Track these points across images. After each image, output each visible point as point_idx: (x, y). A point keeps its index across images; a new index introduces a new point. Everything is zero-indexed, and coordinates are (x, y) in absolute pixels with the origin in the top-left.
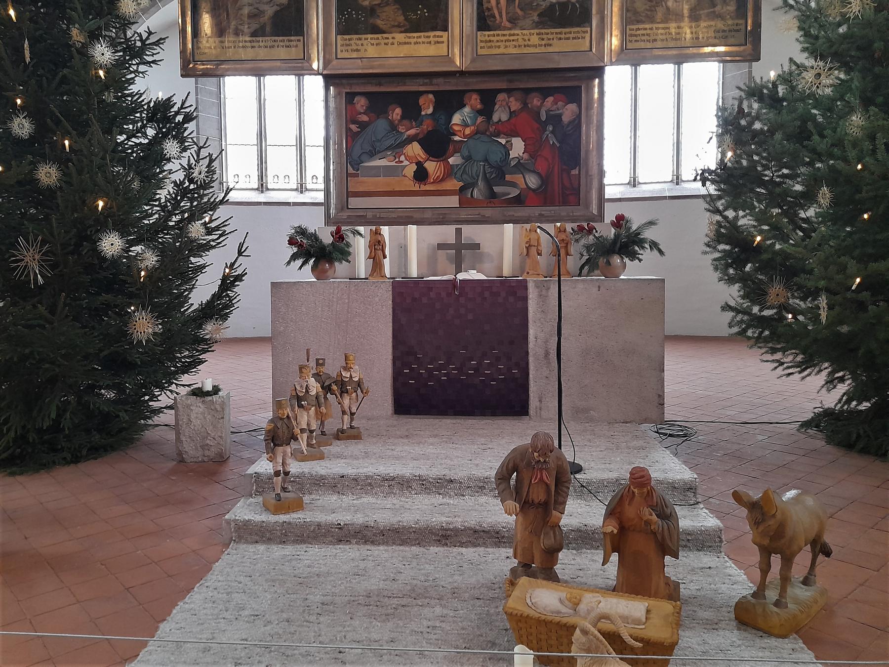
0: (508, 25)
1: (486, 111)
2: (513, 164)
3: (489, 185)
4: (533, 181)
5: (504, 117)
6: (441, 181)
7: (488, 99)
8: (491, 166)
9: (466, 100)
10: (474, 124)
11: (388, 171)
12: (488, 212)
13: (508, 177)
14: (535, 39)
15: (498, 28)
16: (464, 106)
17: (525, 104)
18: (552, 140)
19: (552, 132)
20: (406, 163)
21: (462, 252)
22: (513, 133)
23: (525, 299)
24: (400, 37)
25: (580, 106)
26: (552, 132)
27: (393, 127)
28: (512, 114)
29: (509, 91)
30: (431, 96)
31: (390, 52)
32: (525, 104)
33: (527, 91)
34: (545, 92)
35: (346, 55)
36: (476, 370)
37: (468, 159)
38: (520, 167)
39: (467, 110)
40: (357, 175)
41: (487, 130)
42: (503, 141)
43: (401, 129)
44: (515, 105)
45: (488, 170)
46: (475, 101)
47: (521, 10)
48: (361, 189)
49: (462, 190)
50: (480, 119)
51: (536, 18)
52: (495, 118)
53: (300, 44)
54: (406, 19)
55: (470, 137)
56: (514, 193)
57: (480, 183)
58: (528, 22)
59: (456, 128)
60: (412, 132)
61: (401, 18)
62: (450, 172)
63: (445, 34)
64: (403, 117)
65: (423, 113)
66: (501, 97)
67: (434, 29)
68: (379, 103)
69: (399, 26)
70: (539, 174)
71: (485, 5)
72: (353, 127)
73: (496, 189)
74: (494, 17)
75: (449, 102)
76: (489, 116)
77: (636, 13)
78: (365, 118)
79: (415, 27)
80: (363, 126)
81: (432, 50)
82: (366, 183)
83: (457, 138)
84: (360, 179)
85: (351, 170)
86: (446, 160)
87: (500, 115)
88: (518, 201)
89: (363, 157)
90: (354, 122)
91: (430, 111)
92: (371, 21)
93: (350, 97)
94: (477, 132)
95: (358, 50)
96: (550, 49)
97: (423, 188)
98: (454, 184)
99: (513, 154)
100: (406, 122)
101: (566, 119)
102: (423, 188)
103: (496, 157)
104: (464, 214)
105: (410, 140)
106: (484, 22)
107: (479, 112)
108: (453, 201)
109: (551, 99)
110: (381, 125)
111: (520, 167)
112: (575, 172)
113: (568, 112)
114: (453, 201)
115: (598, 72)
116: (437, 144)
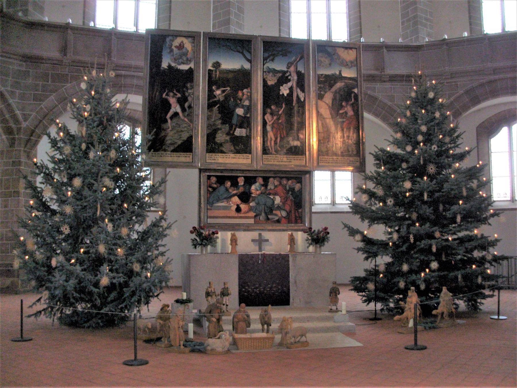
0: (275, 153)
2: (276, 206)
3: (266, 214)
4: (284, 214)
5: (273, 188)
6: (247, 212)
7: (266, 180)
8: (267, 207)
9: (257, 180)
10: (260, 189)
13: (274, 212)
14: (285, 159)
15: (271, 154)
18: (291, 197)
19: (292, 194)
20: (232, 205)
21: (260, 242)
22: (276, 194)
23: (288, 261)
24: (232, 155)
25: (301, 185)
26: (292, 194)
27: (227, 190)
28: (276, 187)
29: (274, 178)
30: (243, 178)
31: (228, 161)
32: (280, 183)
33: (281, 178)
34: (288, 179)
35: (210, 161)
36: (271, 288)
37: (258, 204)
38: (279, 208)
39: (257, 184)
40: (211, 209)
41: (266, 193)
42: (272, 197)
43: (230, 190)
45: (266, 208)
46: (260, 181)
47: (280, 147)
48: (212, 215)
49: (256, 216)
50: (263, 188)
51: (285, 151)
52: (269, 188)
53: (191, 156)
54: (235, 149)
55: (259, 195)
56: (276, 218)
57: (263, 214)
58: (282, 152)
59: (253, 191)
60: (235, 192)
61: (233, 148)
62: (251, 209)
63: (250, 155)
64: (231, 186)
65: (239, 184)
66: (271, 180)
67: (246, 153)
68: (221, 180)
69: (232, 151)
70: (287, 211)
71: (266, 145)
72: (210, 189)
73: (270, 217)
74: (269, 149)
75: (250, 181)
77: (322, 152)
78: (215, 186)
79: (238, 152)
80: (214, 189)
81: (245, 161)
82: (216, 213)
83: (253, 195)
84: (213, 211)
85: (209, 207)
86: (249, 203)
87: (270, 186)
88: (278, 221)
89: (215, 201)
90: (210, 187)
91: (242, 184)
92: (221, 148)
93: (209, 177)
94: (261, 193)
95: (215, 160)
96: (291, 163)
97: (240, 215)
98: (252, 214)
99: (276, 202)
100: (232, 188)
102: (240, 215)
103: (269, 203)
106: (265, 151)
107: (263, 185)
108: (252, 221)
109: (290, 181)
110: (222, 189)
111: (279, 208)
112: (300, 210)
113: (297, 187)
114: (252, 221)
115: (309, 173)
116: (245, 197)
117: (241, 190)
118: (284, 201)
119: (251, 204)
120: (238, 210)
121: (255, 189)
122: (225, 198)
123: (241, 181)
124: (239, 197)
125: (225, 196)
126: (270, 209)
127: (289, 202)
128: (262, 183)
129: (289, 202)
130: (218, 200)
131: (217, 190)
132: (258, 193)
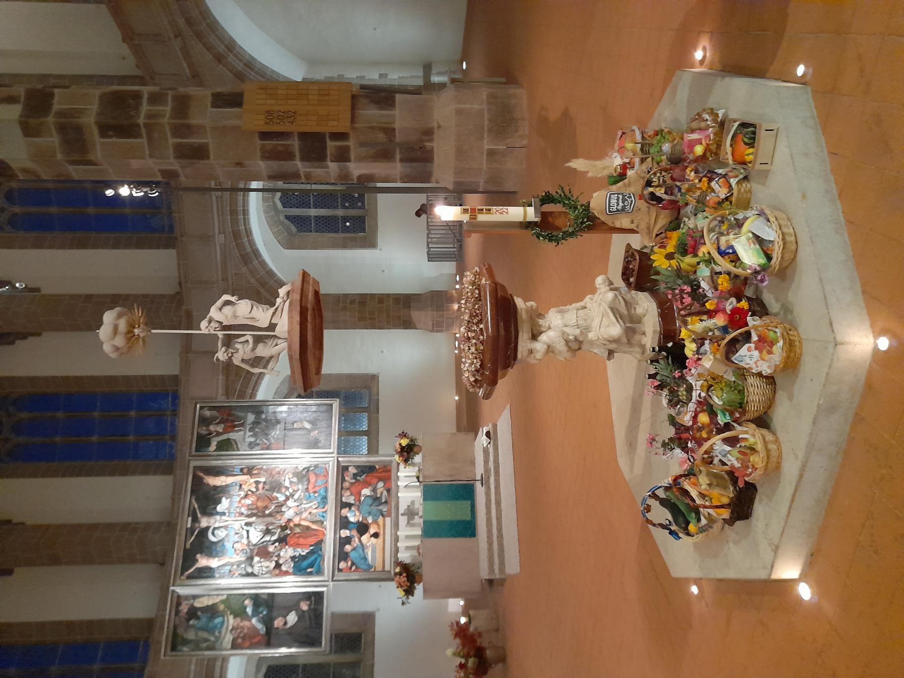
1: (349, 505)
4: (381, 484)
5: (353, 498)
11: (374, 551)
12: (393, 504)
16: (346, 517)
17: (348, 489)
18: (363, 477)
22: (359, 494)
28: (351, 494)
32: (348, 489)
34: (343, 480)
37: (370, 513)
38: (374, 490)
39: (348, 515)
41: (359, 505)
42: (363, 498)
44: (348, 493)
46: (345, 512)
49: (383, 516)
50: (353, 508)
52: (353, 502)
56: (385, 493)
57: (381, 507)
60: (357, 540)
62: (375, 522)
64: (350, 544)
66: (344, 500)
72: (354, 568)
73: (383, 500)
75: (344, 523)
76: (352, 505)
78: (350, 563)
80: (353, 564)
87: (351, 500)
88: (389, 491)
91: (348, 531)
99: (369, 494)
101: (355, 471)
103: (370, 501)
104: (393, 515)
105: (360, 541)
110: (353, 555)
111: (374, 490)
112: (377, 467)
114: (388, 520)
116: (362, 528)
117: (354, 533)
118: (367, 484)
119: (370, 521)
120: (376, 535)
121: (353, 517)
122: (363, 550)
123: (345, 533)
124: (361, 536)
125: (361, 550)
126: (376, 499)
127: (369, 479)
128: (347, 509)
129: (369, 479)
130: (365, 559)
131: (355, 561)
132: (358, 514)
